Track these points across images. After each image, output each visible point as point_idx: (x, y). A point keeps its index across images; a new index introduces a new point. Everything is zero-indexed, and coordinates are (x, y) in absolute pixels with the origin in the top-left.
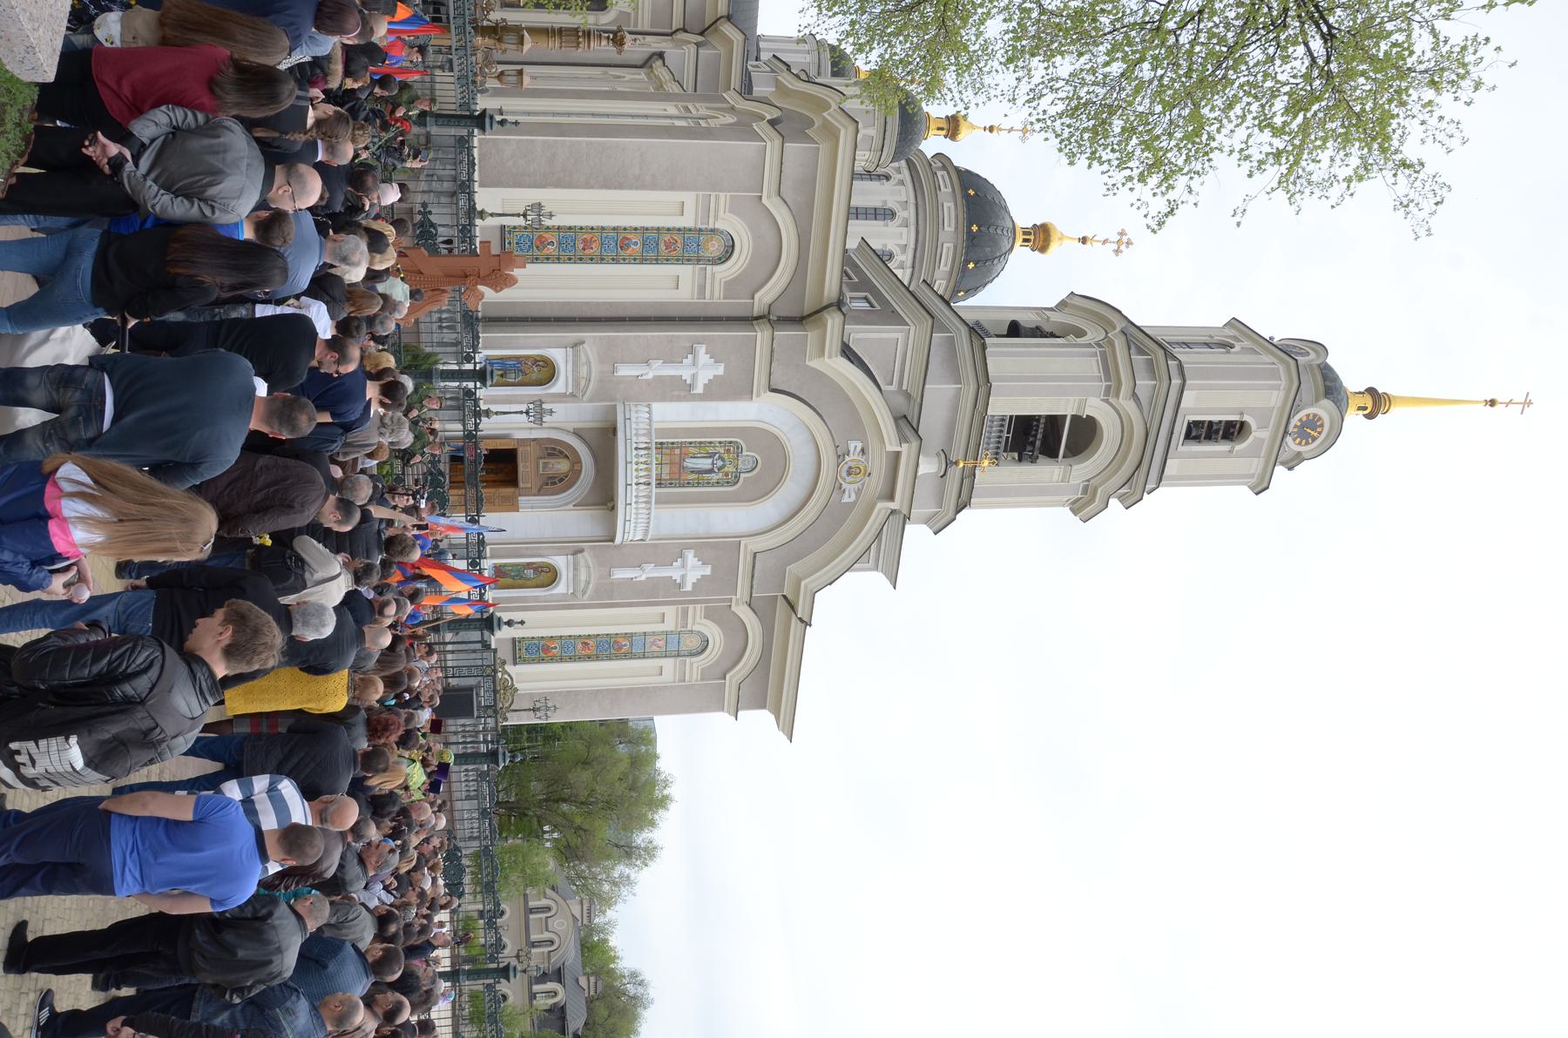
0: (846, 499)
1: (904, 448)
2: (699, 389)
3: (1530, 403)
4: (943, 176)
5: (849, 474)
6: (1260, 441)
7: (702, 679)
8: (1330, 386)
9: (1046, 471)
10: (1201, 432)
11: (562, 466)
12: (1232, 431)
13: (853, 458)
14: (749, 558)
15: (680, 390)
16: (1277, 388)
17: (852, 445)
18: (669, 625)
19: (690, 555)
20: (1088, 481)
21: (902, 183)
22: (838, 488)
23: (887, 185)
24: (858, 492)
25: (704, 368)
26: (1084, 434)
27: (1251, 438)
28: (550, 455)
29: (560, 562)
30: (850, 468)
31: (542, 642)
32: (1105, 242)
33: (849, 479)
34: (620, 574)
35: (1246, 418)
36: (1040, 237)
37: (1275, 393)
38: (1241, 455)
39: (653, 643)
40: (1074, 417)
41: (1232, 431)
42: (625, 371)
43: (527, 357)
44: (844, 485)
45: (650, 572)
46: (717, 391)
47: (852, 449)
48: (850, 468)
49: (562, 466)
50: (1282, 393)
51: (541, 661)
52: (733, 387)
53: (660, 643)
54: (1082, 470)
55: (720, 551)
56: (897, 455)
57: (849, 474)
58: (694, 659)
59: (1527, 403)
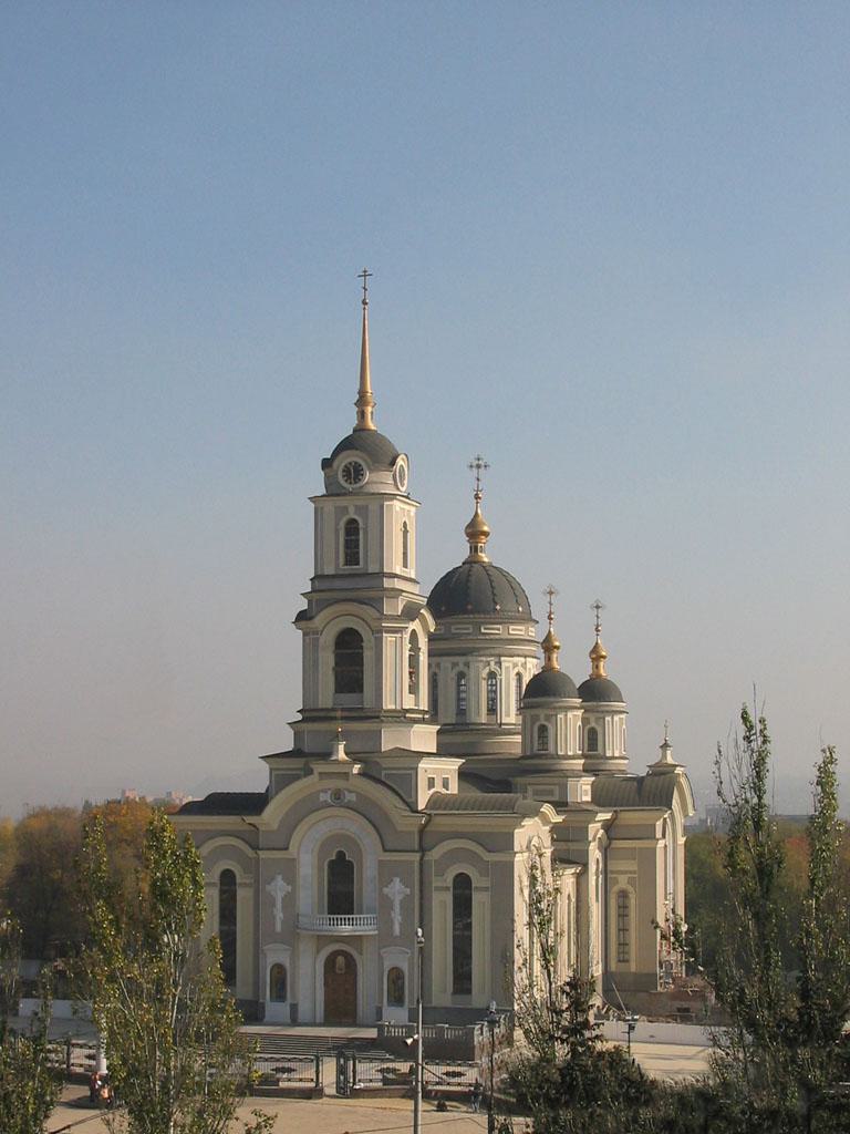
0: (354, 799)
1: (315, 772)
2: (289, 888)
5: (339, 799)
6: (358, 509)
10: (352, 556)
11: (340, 960)
13: (325, 797)
14: (387, 854)
15: (290, 900)
17: (321, 799)
19: (386, 890)
22: (348, 807)
24: (350, 792)
25: (279, 888)
27: (356, 517)
28: (334, 966)
29: (387, 966)
34: (397, 930)
38: (366, 518)
42: (278, 928)
45: (397, 918)
46: (291, 879)
49: (340, 960)
52: (289, 870)
55: (386, 873)
56: (320, 773)
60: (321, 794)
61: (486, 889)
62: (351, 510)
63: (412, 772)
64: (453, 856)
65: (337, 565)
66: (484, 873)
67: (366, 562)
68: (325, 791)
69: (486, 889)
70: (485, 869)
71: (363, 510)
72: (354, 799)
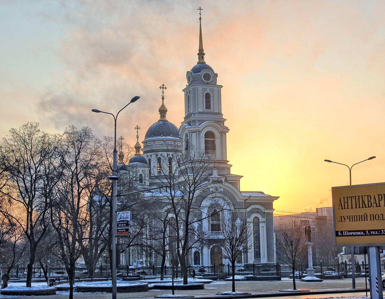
0: (222, 190)
3: (200, 8)
4: (148, 144)
5: (217, 190)
7: (265, 217)
8: (196, 70)
9: (218, 142)
11: (216, 250)
12: (208, 96)
16: (197, 88)
18: (252, 225)
20: (219, 132)
21: (151, 156)
23: (152, 159)
26: (209, 135)
30: (216, 190)
31: (255, 253)
32: (163, 92)
33: (218, 190)
35: (205, 95)
36: (163, 111)
37: (199, 88)
38: (213, 94)
39: (256, 229)
40: (205, 138)
41: (208, 96)
43: (194, 257)
44: (220, 191)
47: (212, 190)
48: (216, 190)
50: (199, 86)
51: (260, 253)
53: (256, 227)
54: (217, 134)
57: (217, 190)
58: (260, 219)
59: (200, 9)
60: (211, 189)
61: (264, 222)
62: (208, 89)
63: (238, 182)
64: (252, 212)
65: (203, 109)
66: (263, 217)
67: (214, 109)
68: (212, 188)
69: (264, 222)
70: (263, 214)
71: (212, 90)
72: (222, 190)
